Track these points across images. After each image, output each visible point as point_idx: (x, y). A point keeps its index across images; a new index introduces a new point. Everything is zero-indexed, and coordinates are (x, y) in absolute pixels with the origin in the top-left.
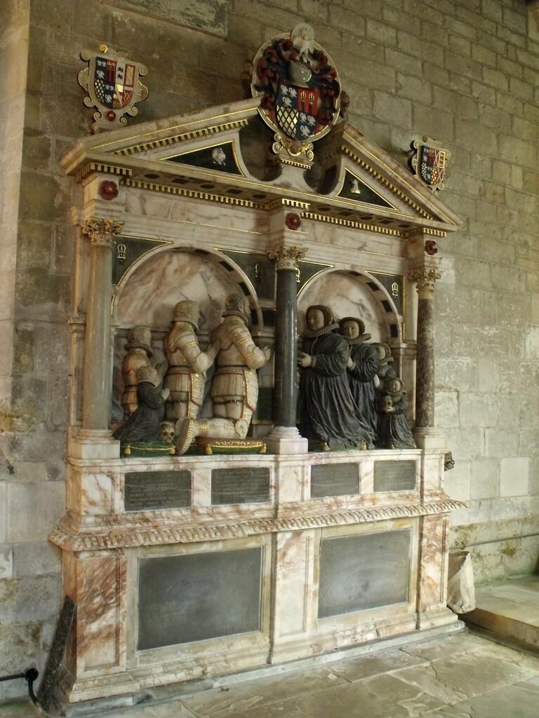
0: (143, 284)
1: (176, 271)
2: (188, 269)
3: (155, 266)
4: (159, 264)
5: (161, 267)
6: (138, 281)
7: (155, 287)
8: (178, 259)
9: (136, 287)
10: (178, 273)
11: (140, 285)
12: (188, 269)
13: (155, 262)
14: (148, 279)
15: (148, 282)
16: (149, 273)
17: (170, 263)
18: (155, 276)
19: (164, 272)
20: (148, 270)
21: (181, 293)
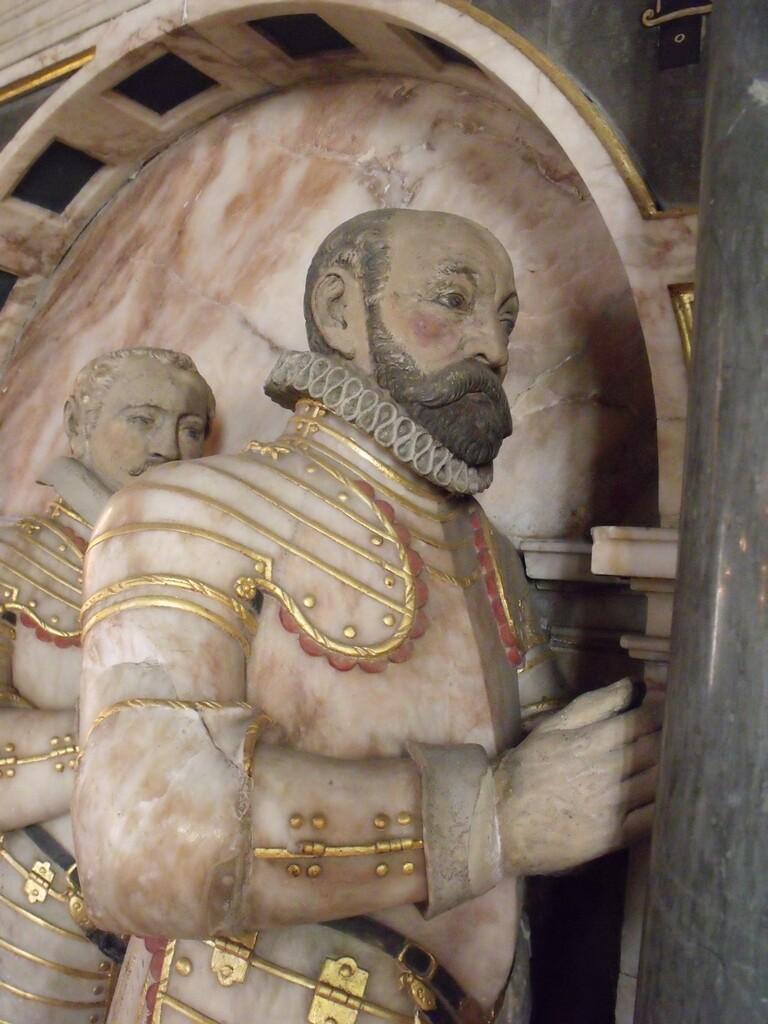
0: (95, 320)
1: (233, 208)
2: (294, 176)
3: (147, 217)
4: (166, 201)
5: (173, 211)
6: (78, 311)
7: (137, 321)
8: (252, 141)
9: (68, 340)
10: (245, 216)
11: (85, 327)
12: (294, 176)
13: (149, 199)
14: (111, 293)
15: (113, 304)
16: (123, 259)
17: (211, 174)
18: (141, 264)
19: (181, 233)
20: (120, 242)
21: (245, 323)
